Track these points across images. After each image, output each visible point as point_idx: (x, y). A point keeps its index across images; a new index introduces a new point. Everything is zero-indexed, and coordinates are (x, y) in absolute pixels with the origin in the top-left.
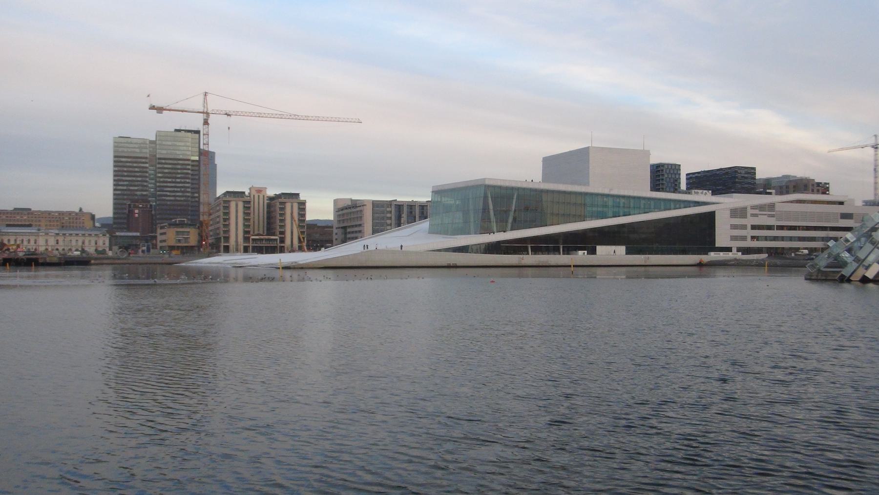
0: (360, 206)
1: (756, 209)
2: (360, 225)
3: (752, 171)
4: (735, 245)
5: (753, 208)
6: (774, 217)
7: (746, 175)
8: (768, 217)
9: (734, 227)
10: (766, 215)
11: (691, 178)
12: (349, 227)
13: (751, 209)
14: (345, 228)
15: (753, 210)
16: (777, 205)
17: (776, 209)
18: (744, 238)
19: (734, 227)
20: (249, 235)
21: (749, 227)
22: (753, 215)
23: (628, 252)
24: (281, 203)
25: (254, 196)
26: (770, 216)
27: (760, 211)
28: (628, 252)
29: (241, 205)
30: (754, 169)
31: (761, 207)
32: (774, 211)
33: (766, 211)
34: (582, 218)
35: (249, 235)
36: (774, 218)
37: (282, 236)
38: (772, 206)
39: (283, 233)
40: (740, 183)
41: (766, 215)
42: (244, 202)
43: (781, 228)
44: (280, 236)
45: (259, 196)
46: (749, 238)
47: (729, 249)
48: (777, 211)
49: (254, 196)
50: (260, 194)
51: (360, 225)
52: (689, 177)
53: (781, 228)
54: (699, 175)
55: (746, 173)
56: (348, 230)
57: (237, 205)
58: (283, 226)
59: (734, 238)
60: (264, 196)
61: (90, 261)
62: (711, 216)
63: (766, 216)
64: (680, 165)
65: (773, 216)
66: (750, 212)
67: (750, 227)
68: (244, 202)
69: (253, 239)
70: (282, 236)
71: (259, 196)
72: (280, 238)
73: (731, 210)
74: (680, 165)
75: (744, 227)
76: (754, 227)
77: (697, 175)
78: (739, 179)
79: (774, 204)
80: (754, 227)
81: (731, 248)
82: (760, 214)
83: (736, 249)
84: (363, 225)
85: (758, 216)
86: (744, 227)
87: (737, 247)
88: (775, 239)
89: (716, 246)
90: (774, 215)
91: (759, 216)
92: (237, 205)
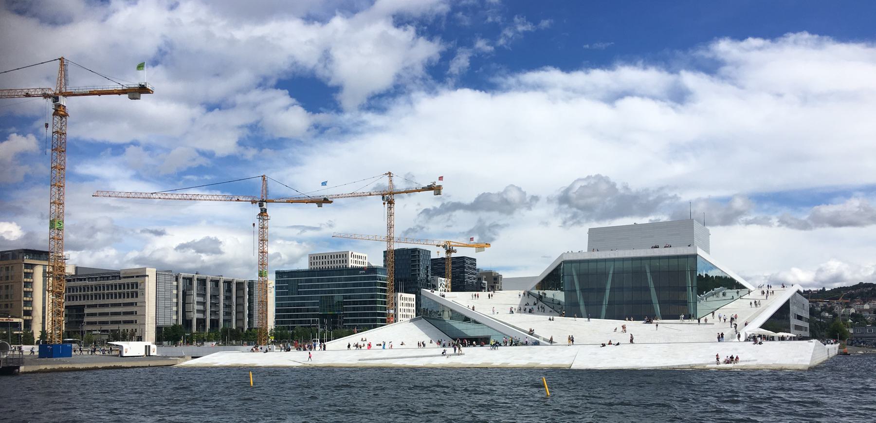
0: (133, 277)
2: (131, 304)
3: (474, 262)
7: (470, 266)
12: (89, 306)
14: (81, 308)
30: (475, 260)
37: (28, 318)
39: (28, 313)
40: (467, 273)
51: (131, 304)
55: (471, 264)
56: (87, 311)
58: (29, 303)
61: (18, 368)
64: (430, 251)
70: (28, 318)
72: (25, 321)
74: (430, 251)
78: (467, 269)
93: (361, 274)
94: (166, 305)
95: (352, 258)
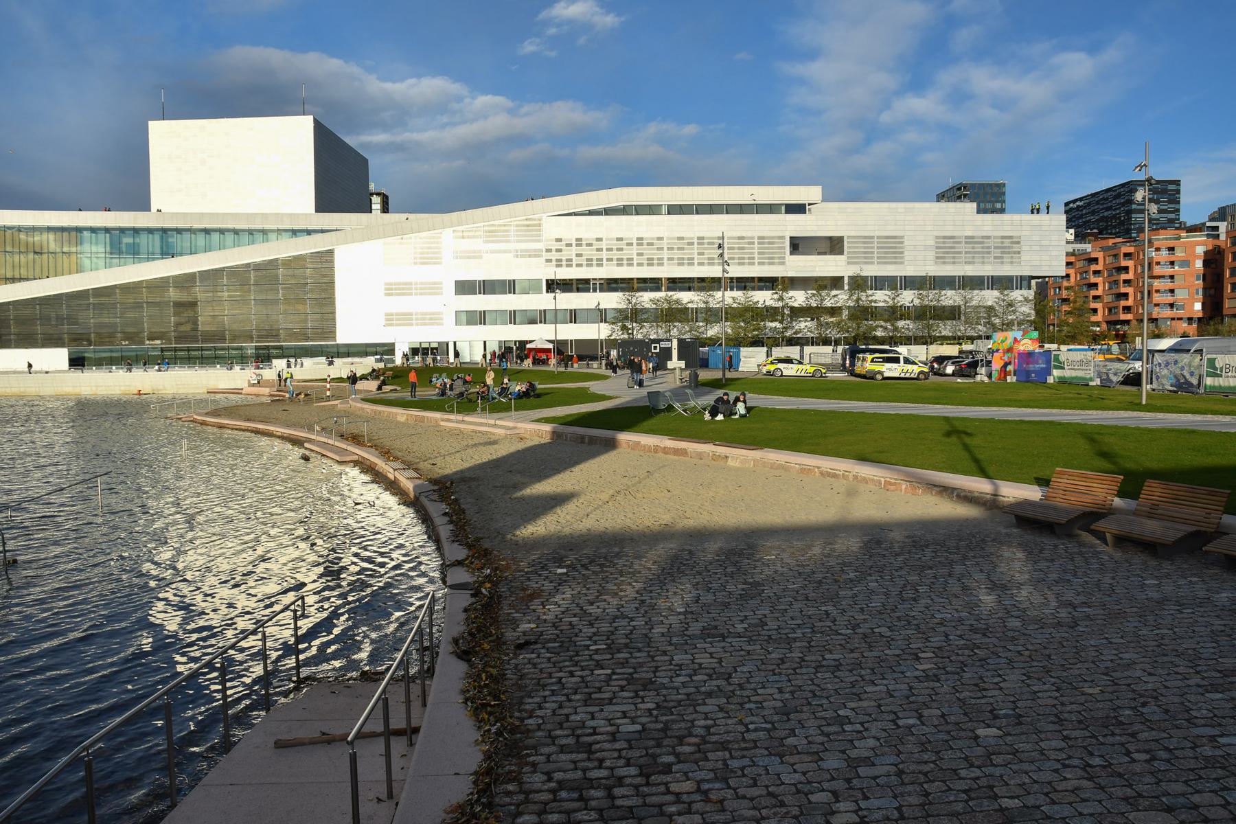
1: (479, 237)
10: (510, 252)
11: (1071, 209)
23: (77, 362)
28: (77, 362)
41: (510, 252)
52: (1068, 208)
53: (552, 285)
59: (391, 320)
65: (535, 254)
76: (464, 288)
77: (1078, 203)
80: (464, 288)
82: (493, 252)
85: (481, 257)
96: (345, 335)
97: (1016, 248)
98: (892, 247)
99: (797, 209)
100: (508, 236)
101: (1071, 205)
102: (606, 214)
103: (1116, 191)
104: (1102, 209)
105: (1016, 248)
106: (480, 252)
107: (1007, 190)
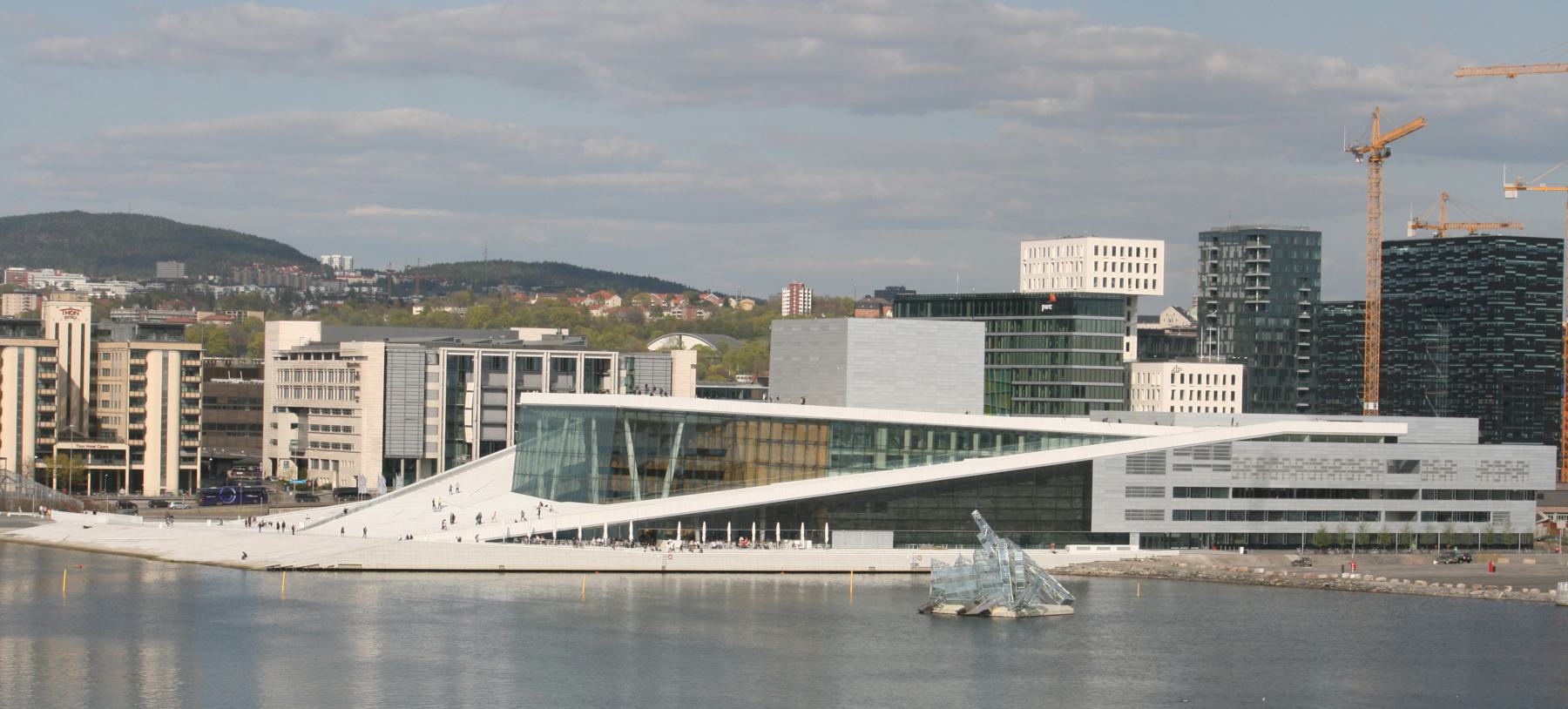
1: (1188, 454)
4: (1136, 528)
5: (1180, 452)
6: (1229, 470)
8: (1213, 470)
9: (1133, 492)
11: (1394, 257)
13: (1175, 454)
15: (1177, 457)
16: (1235, 446)
17: (1234, 455)
18: (1157, 515)
19: (1133, 492)
20: (53, 441)
21: (1169, 492)
22: (1178, 467)
24: (137, 353)
25: (57, 325)
26: (1217, 468)
27: (1195, 458)
29: (30, 355)
31: (1201, 452)
32: (1229, 459)
33: (1208, 459)
34: (817, 470)
35: (53, 441)
36: (1229, 474)
38: (1222, 450)
39: (138, 434)
42: (41, 351)
43: (1238, 493)
44: (131, 442)
45: (70, 325)
46: (1169, 515)
47: (1122, 539)
48: (1235, 458)
49: (57, 325)
50: (70, 321)
52: (1388, 252)
53: (1238, 493)
54: (1413, 251)
57: (21, 358)
59: (1132, 515)
60: (83, 326)
62: (1085, 468)
63: (1211, 469)
64: (1317, 235)
65: (1227, 468)
66: (1171, 460)
67: (1172, 492)
68: (41, 351)
69: (60, 451)
71: (70, 325)
72: (133, 448)
73: (1128, 457)
74: (1317, 235)
75: (1158, 492)
76: (1180, 492)
79: (1230, 443)
80: (1180, 492)
81: (1128, 534)
83: (1138, 536)
84: (356, 413)
85: (1190, 470)
86: (1158, 492)
87: (1141, 534)
88: (1234, 516)
89: (1093, 530)
90: (1229, 466)
91: (1194, 469)
92: (21, 358)
93: (1047, 312)
94: (407, 415)
95: (1101, 258)
96: (1097, 526)
97: (1526, 470)
98: (1449, 471)
99: (1391, 439)
100: (1208, 454)
101: (1394, 249)
102: (1272, 440)
103: (1472, 245)
104: (1449, 270)
105: (1526, 470)
106: (1190, 465)
107: (1325, 242)
